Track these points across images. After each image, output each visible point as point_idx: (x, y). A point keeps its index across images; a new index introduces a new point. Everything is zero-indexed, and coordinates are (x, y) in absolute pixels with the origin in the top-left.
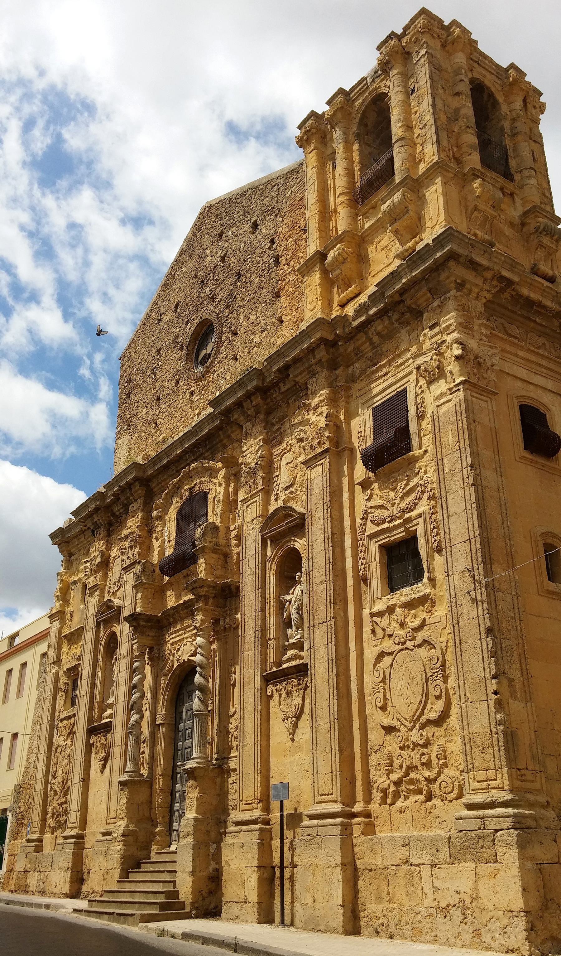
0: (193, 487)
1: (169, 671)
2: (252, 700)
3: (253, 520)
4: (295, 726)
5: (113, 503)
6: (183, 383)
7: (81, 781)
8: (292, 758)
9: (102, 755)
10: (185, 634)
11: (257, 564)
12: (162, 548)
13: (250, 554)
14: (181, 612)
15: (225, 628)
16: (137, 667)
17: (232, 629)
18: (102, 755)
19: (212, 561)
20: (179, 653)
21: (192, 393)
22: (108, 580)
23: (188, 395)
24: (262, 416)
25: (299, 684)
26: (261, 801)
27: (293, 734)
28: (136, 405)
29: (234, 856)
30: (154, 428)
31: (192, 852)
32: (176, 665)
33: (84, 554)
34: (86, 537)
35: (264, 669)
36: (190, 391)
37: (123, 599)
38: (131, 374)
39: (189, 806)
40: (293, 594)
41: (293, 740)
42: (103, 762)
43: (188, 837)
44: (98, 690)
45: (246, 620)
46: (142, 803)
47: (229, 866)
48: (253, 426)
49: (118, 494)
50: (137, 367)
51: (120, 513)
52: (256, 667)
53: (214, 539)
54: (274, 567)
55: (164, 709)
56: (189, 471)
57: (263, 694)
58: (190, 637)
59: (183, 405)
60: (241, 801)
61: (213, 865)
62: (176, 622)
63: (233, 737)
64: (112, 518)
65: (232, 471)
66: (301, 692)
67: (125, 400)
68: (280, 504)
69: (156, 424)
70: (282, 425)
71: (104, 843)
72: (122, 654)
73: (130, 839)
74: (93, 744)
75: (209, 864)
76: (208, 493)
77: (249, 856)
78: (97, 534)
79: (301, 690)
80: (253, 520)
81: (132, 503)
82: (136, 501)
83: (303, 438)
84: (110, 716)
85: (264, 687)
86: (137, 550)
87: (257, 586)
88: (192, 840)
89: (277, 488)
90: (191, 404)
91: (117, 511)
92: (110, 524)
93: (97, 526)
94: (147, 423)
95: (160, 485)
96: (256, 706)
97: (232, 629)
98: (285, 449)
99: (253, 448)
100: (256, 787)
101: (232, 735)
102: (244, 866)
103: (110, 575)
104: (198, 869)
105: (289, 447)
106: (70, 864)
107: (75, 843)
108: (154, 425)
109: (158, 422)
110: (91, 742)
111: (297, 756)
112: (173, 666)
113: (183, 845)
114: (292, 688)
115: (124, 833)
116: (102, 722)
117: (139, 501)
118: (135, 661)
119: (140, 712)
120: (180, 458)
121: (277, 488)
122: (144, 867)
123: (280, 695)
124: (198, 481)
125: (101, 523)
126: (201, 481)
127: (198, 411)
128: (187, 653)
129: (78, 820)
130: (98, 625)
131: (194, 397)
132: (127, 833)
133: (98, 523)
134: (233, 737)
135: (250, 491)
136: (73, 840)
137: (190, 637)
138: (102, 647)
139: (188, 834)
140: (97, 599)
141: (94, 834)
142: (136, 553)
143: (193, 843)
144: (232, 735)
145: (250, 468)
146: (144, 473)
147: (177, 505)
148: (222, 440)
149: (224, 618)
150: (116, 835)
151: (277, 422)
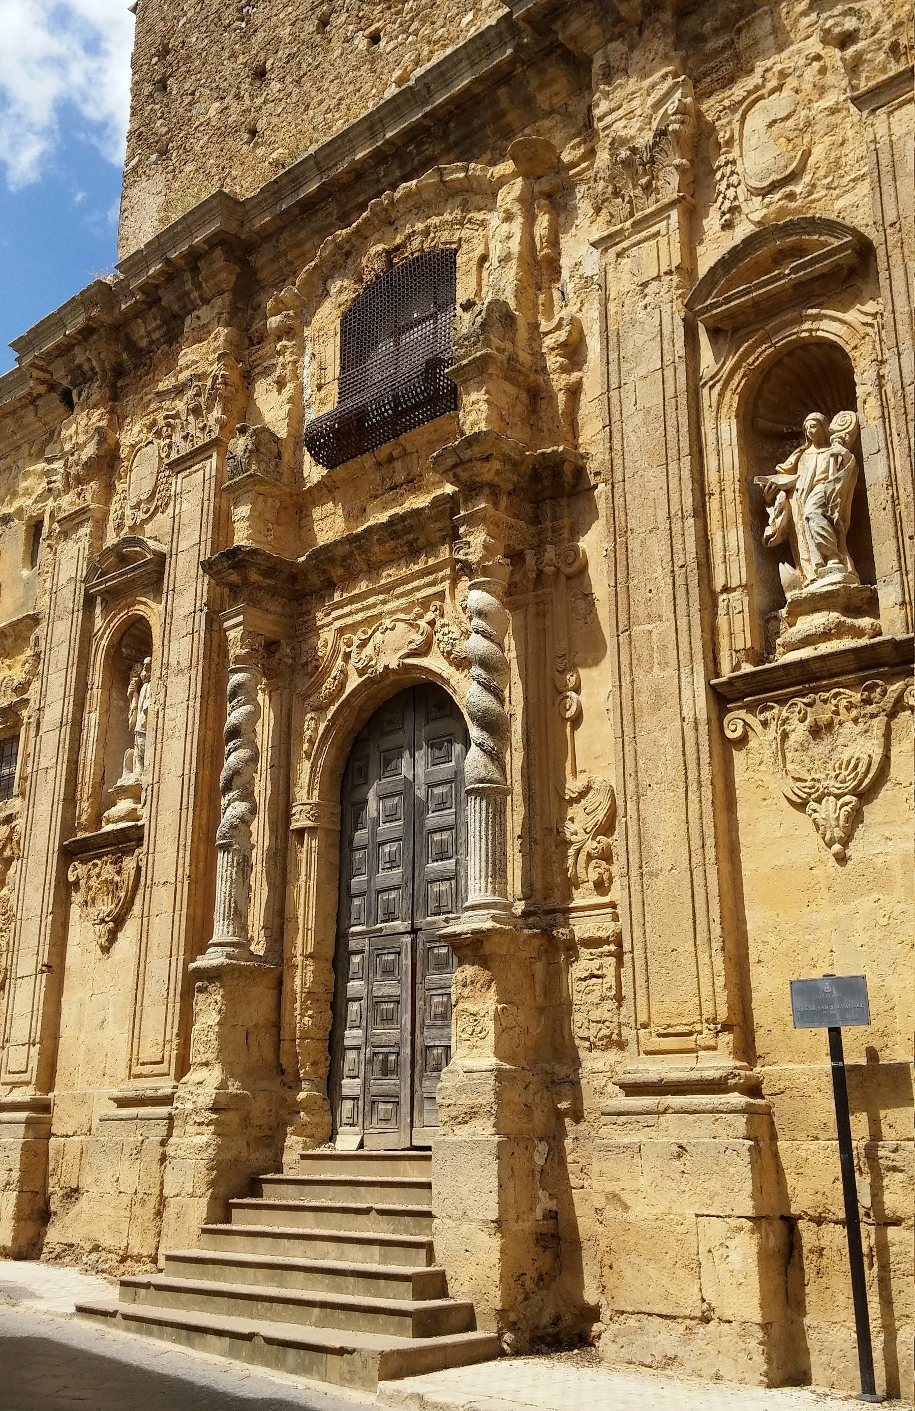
0: (397, 248)
1: (332, 698)
2: (672, 753)
3: (645, 285)
4: (855, 818)
5: (137, 313)
6: (343, 19)
7: (43, 972)
8: (843, 910)
9: (106, 906)
10: (384, 602)
11: (670, 393)
12: (297, 405)
13: (642, 371)
14: (376, 549)
15: (540, 573)
16: (239, 686)
17: (563, 579)
18: (106, 909)
19: (503, 402)
20: (369, 650)
21: (375, 39)
22: (115, 498)
23: (361, 42)
24: (667, 17)
25: (867, 702)
26: (727, 1027)
27: (845, 842)
28: (187, 99)
29: (643, 1181)
30: (248, 143)
31: (495, 1166)
32: (354, 682)
33: (30, 455)
34: (41, 412)
35: (713, 665)
36: (367, 32)
37: (175, 531)
38: (171, 32)
39: (465, 1036)
40: (794, 470)
41: (842, 859)
42: (111, 924)
43: (473, 1122)
44: (89, 754)
45: (634, 544)
46: (256, 1026)
47: (626, 1208)
48: (632, 48)
49: (157, 286)
50: (189, 15)
51: (152, 342)
52: (684, 660)
53: (509, 345)
54: (732, 401)
55: (316, 792)
56: (392, 203)
57: (716, 735)
58: (406, 610)
59: (343, 70)
60: (645, 1026)
61: (545, 1202)
62: (352, 577)
63: (582, 857)
64: (125, 356)
65: (544, 185)
66: (878, 724)
67: (151, 95)
68: (743, 230)
69: (253, 132)
70: (739, 31)
71: (130, 1125)
72: (173, 662)
73: (233, 1117)
74: (76, 883)
75: (534, 1199)
76: (456, 251)
77: (715, 1184)
78: (80, 395)
79: (873, 716)
80: (645, 285)
81: (194, 309)
82: (206, 301)
83: (856, 31)
84: (132, 815)
85: (714, 717)
86: (217, 413)
87: (673, 453)
88: (493, 1130)
89: (731, 193)
90: (372, 62)
91: (142, 338)
92: (119, 371)
93: (82, 378)
94: (224, 132)
95: (282, 262)
96: (692, 766)
97: (563, 579)
98: (757, 88)
99: (636, 103)
100: (706, 991)
101: (578, 852)
102: (690, 1213)
103: (120, 487)
104: (512, 1214)
105: (770, 85)
106: (15, 1175)
107: (29, 1122)
108: (246, 136)
109: (261, 125)
110: (71, 878)
111: (866, 904)
112: (342, 686)
113: (459, 1145)
114: (837, 713)
115: (216, 1101)
116: (103, 830)
117: (218, 302)
118: (235, 671)
119: (247, 795)
120: (358, 174)
121: (731, 193)
122: (271, 1195)
123: (785, 736)
124: (420, 226)
125: (92, 369)
126: (428, 227)
127: (398, 73)
128: (396, 650)
129: (34, 1064)
130: (89, 602)
131: (382, 43)
132: (223, 1102)
133: (86, 367)
134: (582, 857)
135: (632, 214)
136: (23, 1115)
137: (406, 610)
138: (101, 656)
139: (472, 1114)
140: (85, 542)
141: (83, 1100)
142: (211, 422)
143: (496, 1138)
144: (578, 852)
145: (634, 150)
146: (242, 224)
147: (344, 297)
148: (504, 114)
149: (538, 549)
150: (189, 1106)
151: (716, 31)
